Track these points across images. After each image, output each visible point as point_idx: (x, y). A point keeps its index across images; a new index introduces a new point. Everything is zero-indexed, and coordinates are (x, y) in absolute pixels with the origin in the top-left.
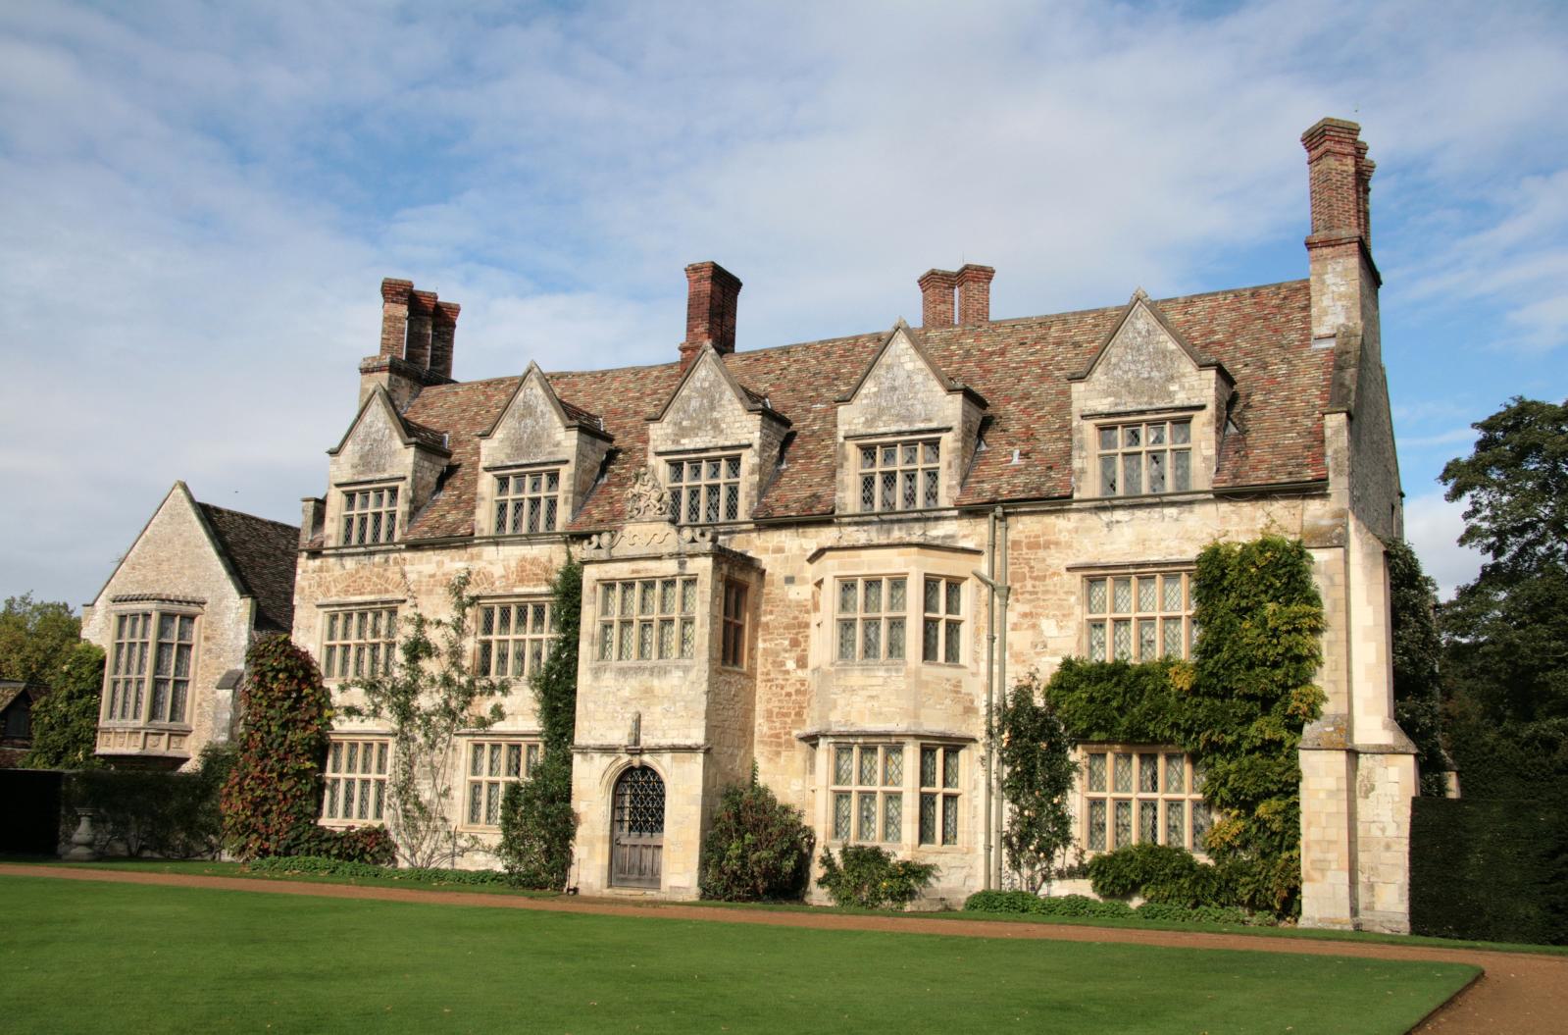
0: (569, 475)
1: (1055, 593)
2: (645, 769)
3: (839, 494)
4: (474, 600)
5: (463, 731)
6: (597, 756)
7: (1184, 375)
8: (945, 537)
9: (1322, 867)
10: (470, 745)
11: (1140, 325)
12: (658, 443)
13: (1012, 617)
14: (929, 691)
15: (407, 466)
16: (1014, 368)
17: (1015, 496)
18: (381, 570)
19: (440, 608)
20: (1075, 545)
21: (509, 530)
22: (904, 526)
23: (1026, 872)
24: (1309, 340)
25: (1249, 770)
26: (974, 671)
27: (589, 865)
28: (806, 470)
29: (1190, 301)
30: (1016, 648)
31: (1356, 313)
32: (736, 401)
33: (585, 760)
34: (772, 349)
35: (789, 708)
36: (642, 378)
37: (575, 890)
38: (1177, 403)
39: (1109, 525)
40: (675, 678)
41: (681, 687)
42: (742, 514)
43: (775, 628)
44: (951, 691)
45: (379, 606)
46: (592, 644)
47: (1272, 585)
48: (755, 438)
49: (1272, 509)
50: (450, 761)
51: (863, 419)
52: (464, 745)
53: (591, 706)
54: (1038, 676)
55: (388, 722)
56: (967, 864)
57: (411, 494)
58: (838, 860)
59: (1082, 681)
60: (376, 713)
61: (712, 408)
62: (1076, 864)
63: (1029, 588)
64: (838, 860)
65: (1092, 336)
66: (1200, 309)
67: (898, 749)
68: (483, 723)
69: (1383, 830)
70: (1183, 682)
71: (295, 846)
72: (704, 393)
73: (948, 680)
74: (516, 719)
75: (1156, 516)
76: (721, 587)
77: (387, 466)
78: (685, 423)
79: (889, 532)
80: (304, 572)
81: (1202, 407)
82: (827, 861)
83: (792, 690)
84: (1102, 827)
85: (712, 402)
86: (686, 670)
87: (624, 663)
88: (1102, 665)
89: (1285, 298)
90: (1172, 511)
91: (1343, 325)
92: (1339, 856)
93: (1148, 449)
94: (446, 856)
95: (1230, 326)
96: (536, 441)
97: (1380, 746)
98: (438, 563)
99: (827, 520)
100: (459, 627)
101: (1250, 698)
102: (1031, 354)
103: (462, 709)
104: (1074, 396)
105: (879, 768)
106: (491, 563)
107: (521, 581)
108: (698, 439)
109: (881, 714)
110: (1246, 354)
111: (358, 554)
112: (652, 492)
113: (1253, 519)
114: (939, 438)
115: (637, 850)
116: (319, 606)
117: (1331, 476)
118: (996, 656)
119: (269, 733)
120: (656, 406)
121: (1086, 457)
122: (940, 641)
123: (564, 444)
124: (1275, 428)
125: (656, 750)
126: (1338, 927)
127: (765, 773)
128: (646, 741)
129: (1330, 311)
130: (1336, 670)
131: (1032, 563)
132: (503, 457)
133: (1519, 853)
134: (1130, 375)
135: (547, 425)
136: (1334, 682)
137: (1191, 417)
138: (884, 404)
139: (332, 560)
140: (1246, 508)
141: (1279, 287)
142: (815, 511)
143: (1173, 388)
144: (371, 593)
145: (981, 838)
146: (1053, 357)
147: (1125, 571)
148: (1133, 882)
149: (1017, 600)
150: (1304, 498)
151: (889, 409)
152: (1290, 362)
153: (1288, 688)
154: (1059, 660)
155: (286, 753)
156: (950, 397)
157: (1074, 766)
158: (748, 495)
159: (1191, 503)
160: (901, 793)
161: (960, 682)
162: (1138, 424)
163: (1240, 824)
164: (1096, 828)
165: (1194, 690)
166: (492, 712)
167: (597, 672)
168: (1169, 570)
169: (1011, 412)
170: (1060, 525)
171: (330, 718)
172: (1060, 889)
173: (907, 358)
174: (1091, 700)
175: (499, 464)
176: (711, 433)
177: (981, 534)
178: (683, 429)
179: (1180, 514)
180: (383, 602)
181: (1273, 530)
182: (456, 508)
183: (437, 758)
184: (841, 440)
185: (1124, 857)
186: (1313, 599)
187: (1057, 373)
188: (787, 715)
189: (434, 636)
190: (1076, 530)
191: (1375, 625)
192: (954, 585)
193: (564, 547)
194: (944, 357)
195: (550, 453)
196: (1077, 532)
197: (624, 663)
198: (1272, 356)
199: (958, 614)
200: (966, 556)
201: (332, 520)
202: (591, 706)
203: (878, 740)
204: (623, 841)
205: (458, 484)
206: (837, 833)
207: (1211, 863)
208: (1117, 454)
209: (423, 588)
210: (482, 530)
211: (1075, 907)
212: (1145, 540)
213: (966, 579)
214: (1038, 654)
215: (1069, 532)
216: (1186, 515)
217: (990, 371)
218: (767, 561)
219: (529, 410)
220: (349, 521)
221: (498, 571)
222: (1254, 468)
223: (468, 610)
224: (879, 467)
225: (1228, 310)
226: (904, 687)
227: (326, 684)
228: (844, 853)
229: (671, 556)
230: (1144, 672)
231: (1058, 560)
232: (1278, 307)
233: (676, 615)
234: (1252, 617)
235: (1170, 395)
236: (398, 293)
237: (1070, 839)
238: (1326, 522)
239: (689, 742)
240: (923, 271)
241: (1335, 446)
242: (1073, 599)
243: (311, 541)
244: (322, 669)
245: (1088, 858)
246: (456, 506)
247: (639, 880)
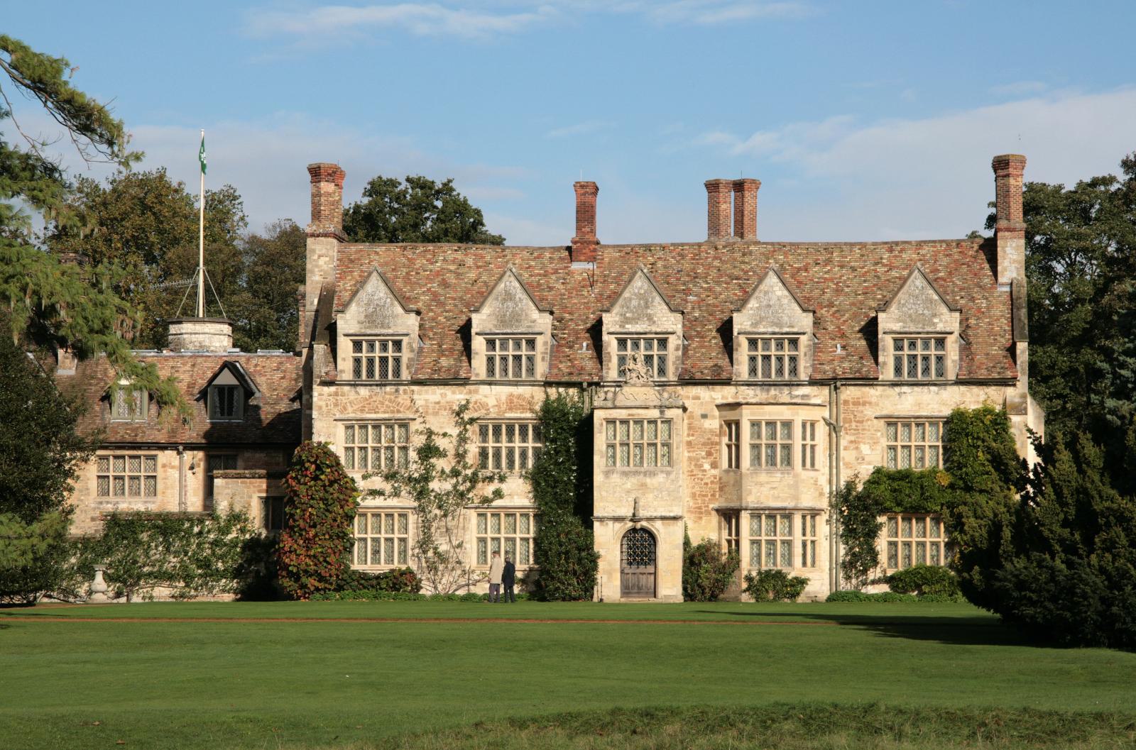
0: (545, 343)
2: (644, 530)
3: (735, 366)
4: (472, 421)
6: (610, 523)
8: (803, 396)
13: (843, 443)
15: (408, 326)
18: (393, 397)
21: (497, 377)
23: (854, 581)
27: (609, 585)
28: (703, 347)
30: (847, 460)
31: (1023, 272)
34: (636, 246)
36: (538, 257)
37: (601, 600)
40: (661, 478)
46: (602, 457)
48: (679, 328)
50: (461, 525)
51: (750, 323)
52: (473, 514)
55: (406, 501)
60: (396, 494)
61: (647, 307)
63: (854, 427)
65: (862, 264)
68: (486, 500)
70: (945, 480)
72: (640, 297)
77: (391, 325)
79: (768, 391)
80: (320, 395)
81: (951, 333)
82: (749, 579)
83: (709, 481)
86: (668, 473)
87: (626, 469)
88: (899, 472)
90: (933, 388)
94: (463, 586)
96: (516, 317)
98: (441, 394)
99: (727, 382)
100: (462, 439)
102: (826, 273)
103: (469, 490)
106: (486, 396)
107: (511, 409)
110: (961, 290)
111: (371, 385)
117: (1019, 374)
118: (834, 464)
120: (563, 283)
123: (540, 321)
124: (986, 342)
125: (649, 519)
128: (642, 513)
132: (491, 326)
139: (346, 388)
140: (975, 389)
143: (936, 320)
144: (385, 412)
145: (828, 564)
146: (841, 276)
154: (871, 469)
156: (805, 314)
158: (674, 363)
159: (945, 385)
162: (917, 338)
164: (893, 557)
166: (493, 493)
167: (607, 474)
168: (933, 421)
170: (872, 393)
175: (488, 331)
178: (627, 318)
181: (988, 402)
182: (443, 355)
187: (846, 290)
188: (706, 496)
189: (441, 443)
190: (881, 396)
192: (813, 425)
193: (543, 388)
198: (976, 293)
201: (344, 359)
202: (604, 494)
204: (626, 571)
205: (431, 335)
209: (430, 411)
210: (477, 375)
211: (884, 598)
219: (509, 296)
220: (357, 361)
221: (491, 402)
222: (979, 367)
224: (760, 352)
228: (760, 573)
229: (655, 407)
230: (922, 476)
231: (870, 412)
232: (975, 257)
233: (659, 442)
235: (934, 324)
238: (1017, 400)
240: (712, 177)
242: (879, 434)
243: (327, 373)
245: (889, 574)
246: (442, 353)
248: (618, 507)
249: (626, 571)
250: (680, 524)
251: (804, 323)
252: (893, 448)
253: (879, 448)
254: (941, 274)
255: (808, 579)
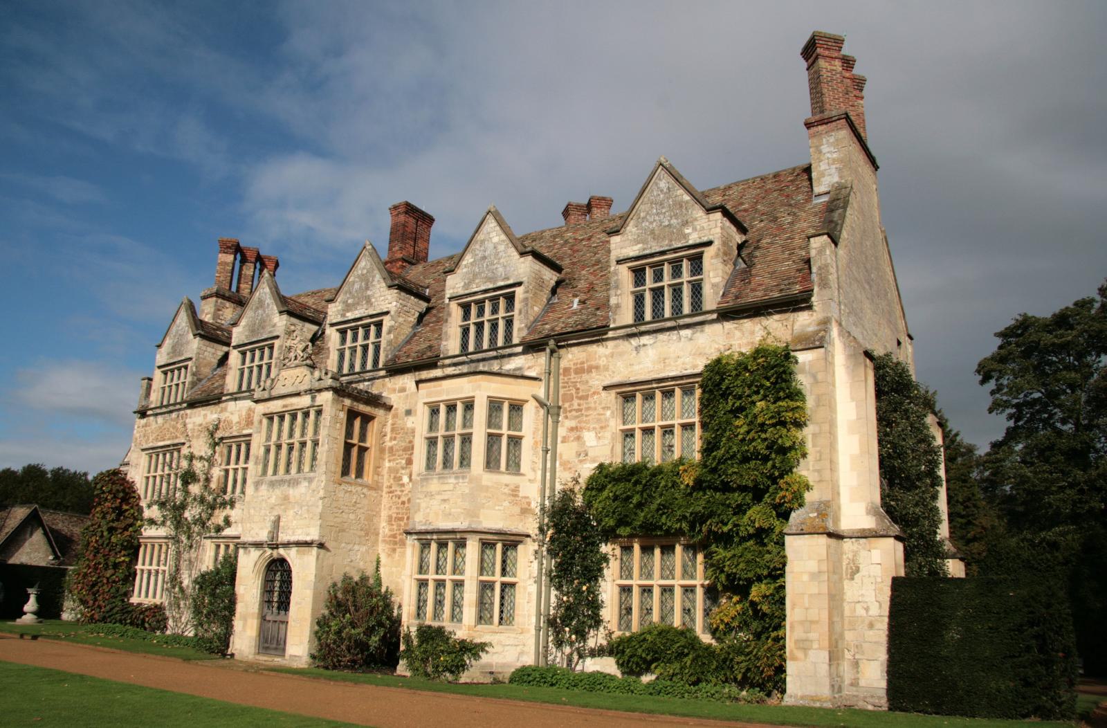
1: (595, 409)
2: (282, 561)
3: (444, 343)
5: (208, 535)
6: (252, 550)
7: (696, 219)
8: (514, 370)
9: (804, 646)
10: (213, 546)
11: (663, 184)
12: (332, 318)
13: (562, 432)
14: (490, 495)
16: (595, 247)
17: (564, 331)
19: (200, 447)
20: (611, 367)
22: (484, 363)
24: (811, 198)
25: (741, 556)
26: (532, 478)
29: (729, 188)
30: (565, 457)
32: (382, 280)
33: (245, 553)
35: (403, 514)
37: (232, 655)
38: (691, 242)
39: (637, 349)
40: (303, 488)
41: (306, 494)
42: (381, 366)
43: (397, 450)
44: (510, 495)
45: (172, 448)
47: (762, 386)
49: (768, 322)
51: (463, 284)
53: (252, 511)
54: (581, 480)
56: (513, 646)
57: (194, 369)
58: (414, 634)
59: (610, 482)
61: (367, 288)
62: (605, 643)
64: (414, 634)
66: (734, 193)
67: (461, 544)
68: (219, 529)
69: (867, 609)
71: (109, 617)
73: (507, 485)
74: (237, 526)
75: (675, 337)
76: (343, 416)
78: (350, 301)
80: (138, 427)
81: (709, 243)
82: (408, 638)
84: (629, 610)
85: (367, 284)
86: (310, 480)
89: (798, 175)
90: (686, 333)
91: (837, 183)
92: (819, 636)
93: (670, 283)
95: (754, 198)
96: (263, 324)
97: (864, 530)
101: (743, 489)
103: (209, 519)
104: (612, 246)
105: (450, 560)
108: (357, 312)
109: (450, 514)
111: (164, 413)
112: (298, 345)
113: (752, 333)
114: (514, 292)
115: (277, 624)
116: (143, 450)
117: (816, 289)
118: (549, 465)
119: (102, 536)
121: (620, 295)
122: (503, 453)
124: (776, 260)
125: (287, 545)
126: (818, 705)
127: (385, 566)
128: (283, 537)
129: (826, 173)
130: (820, 460)
131: (578, 386)
133: (990, 628)
134: (655, 224)
135: (270, 312)
136: (819, 471)
137: (702, 253)
138: (477, 270)
139: (152, 418)
140: (747, 324)
141: (794, 169)
142: (425, 357)
144: (169, 439)
145: (534, 620)
147: (650, 386)
148: (645, 660)
149: (566, 417)
150: (795, 310)
151: (480, 273)
152: (795, 214)
153: (776, 478)
155: (110, 551)
156: (522, 259)
157: (605, 559)
158: (385, 350)
159: (702, 323)
160: (463, 581)
161: (518, 487)
162: (661, 263)
163: (739, 607)
165: (699, 485)
166: (224, 521)
167: (257, 485)
168: (685, 383)
169: (584, 278)
170: (599, 352)
171: (141, 526)
172: (591, 665)
173: (494, 234)
174: (616, 498)
175: (241, 343)
176: (365, 306)
177: (541, 365)
179: (694, 334)
180: (174, 445)
181: (769, 341)
183: (193, 554)
184: (447, 301)
185: (639, 639)
186: (796, 395)
188: (401, 519)
189: (198, 466)
190: (612, 355)
191: (857, 419)
192: (516, 407)
194: (549, 247)
195: (270, 332)
196: (612, 357)
197: (274, 478)
199: (520, 430)
200: (527, 381)
202: (252, 511)
203: (444, 537)
204: (268, 618)
206: (418, 615)
207: (714, 642)
208: (645, 290)
209: (195, 434)
211: (597, 682)
212: (665, 359)
213: (527, 401)
214: (581, 461)
215: (606, 356)
216: (698, 334)
217: (578, 251)
218: (393, 398)
219: (261, 303)
221: (235, 419)
222: (753, 290)
223: (217, 448)
225: (755, 189)
226: (467, 491)
227: (141, 504)
230: (659, 471)
231: (597, 381)
234: (746, 416)
235: (685, 236)
236: (228, 247)
237: (602, 621)
238: (811, 329)
239: (308, 539)
241: (819, 264)
242: (608, 413)
244: (142, 496)
247: (276, 649)
248: (262, 529)
249: (268, 618)
250: (315, 550)
251: (521, 271)
252: (629, 434)
253: (608, 434)
254: (746, 206)
255: (491, 645)
